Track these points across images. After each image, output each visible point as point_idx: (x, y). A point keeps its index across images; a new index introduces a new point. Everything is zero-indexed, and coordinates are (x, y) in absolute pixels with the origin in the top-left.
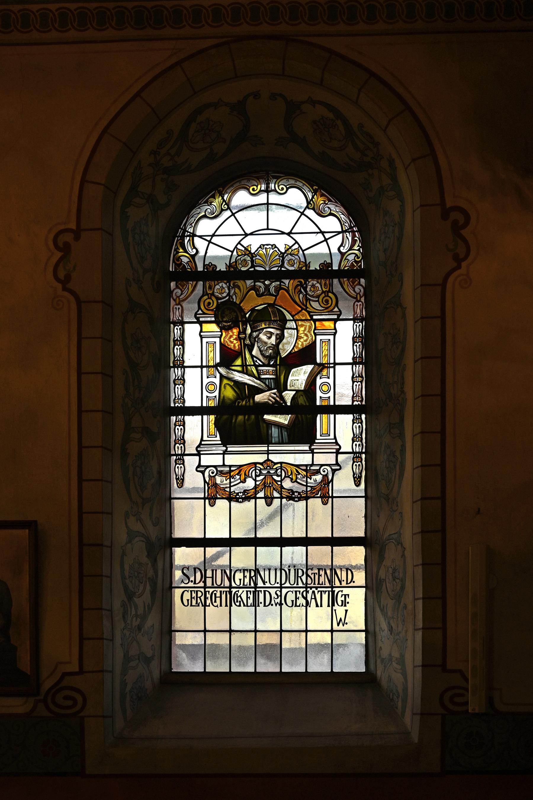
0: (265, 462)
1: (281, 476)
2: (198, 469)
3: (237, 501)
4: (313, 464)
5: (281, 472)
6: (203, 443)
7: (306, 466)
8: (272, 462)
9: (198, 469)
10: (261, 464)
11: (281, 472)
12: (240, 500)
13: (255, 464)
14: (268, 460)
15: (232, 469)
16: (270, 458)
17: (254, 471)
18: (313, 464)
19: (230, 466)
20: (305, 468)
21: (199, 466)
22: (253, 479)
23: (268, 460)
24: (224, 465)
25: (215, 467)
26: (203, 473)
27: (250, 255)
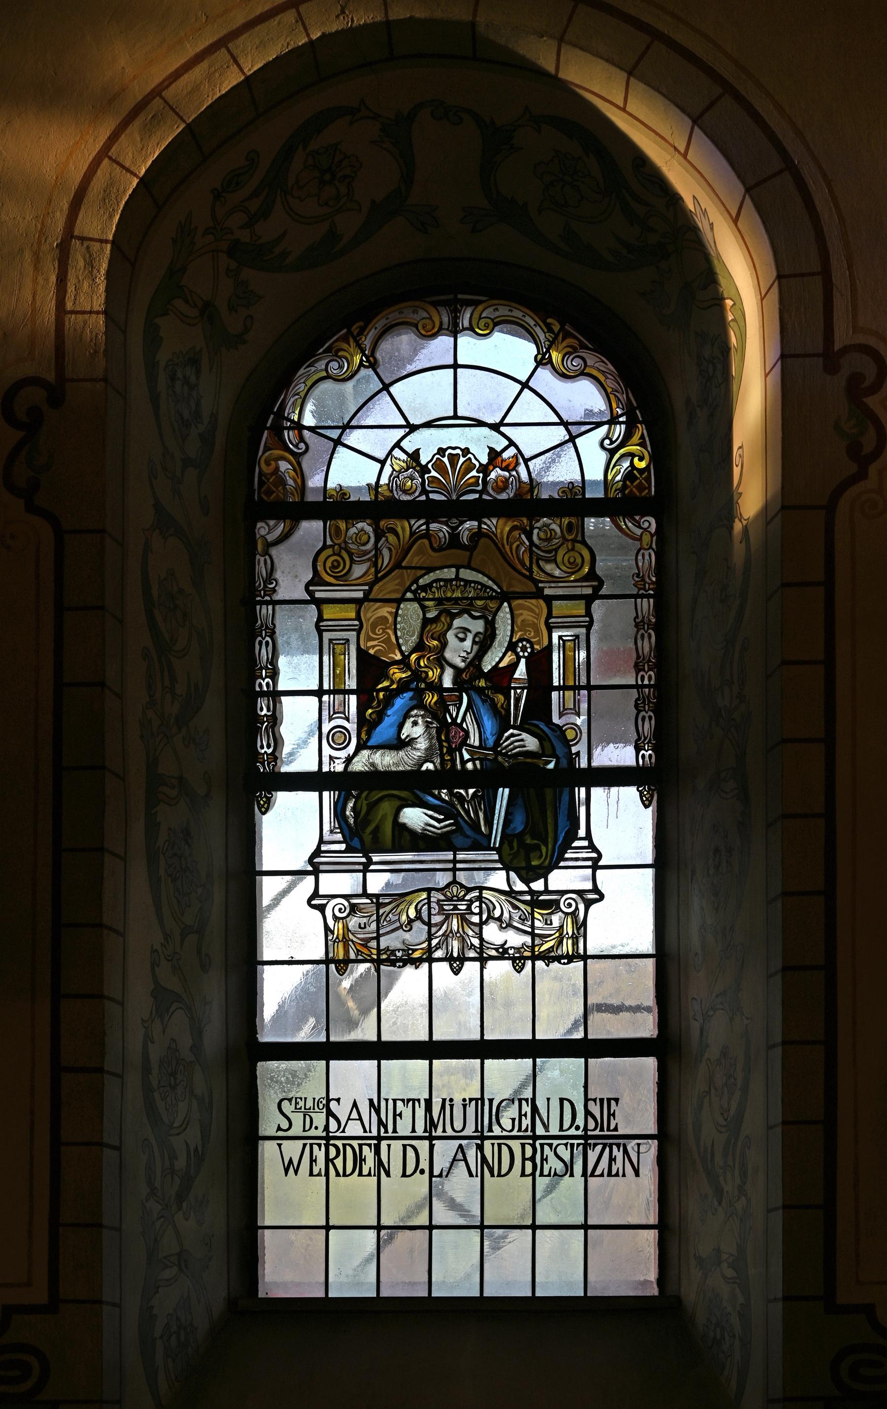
8: (462, 886)
14: (454, 882)
17: (426, 906)
19: (377, 896)
21: (316, 894)
23: (454, 882)
26: (321, 909)
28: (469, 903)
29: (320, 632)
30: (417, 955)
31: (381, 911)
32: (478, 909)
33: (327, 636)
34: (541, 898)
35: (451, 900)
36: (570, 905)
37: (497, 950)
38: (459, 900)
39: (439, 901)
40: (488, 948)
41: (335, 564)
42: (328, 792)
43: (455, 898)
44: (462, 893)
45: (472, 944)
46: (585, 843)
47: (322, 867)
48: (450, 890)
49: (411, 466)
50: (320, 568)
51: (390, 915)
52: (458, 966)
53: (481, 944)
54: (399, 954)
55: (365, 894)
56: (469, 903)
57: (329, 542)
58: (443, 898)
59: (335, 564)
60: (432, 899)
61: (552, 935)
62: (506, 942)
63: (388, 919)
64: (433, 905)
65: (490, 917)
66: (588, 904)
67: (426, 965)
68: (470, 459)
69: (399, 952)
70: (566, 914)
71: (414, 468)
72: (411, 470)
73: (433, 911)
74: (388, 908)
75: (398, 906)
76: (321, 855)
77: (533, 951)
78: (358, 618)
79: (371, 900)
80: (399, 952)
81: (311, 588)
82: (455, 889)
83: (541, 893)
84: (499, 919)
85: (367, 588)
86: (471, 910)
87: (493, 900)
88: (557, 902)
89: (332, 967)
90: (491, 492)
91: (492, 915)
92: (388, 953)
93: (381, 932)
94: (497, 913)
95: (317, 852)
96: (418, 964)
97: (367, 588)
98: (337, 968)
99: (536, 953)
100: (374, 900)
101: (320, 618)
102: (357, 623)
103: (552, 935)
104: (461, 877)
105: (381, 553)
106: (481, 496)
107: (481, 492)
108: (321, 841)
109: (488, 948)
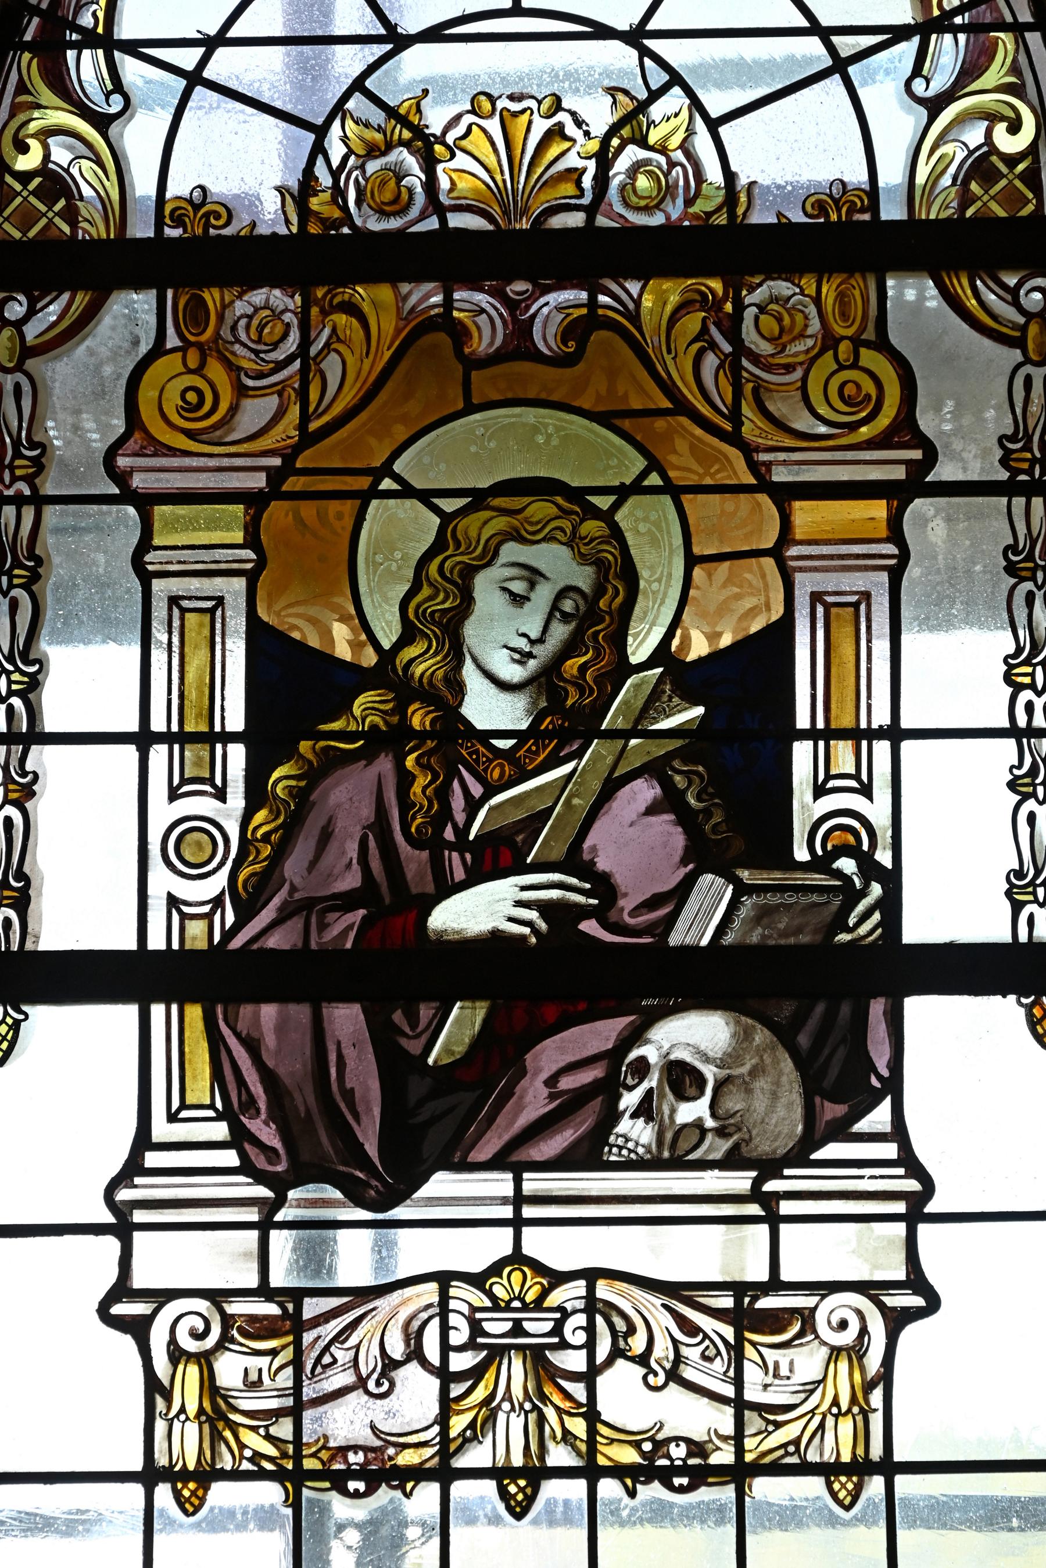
0: (496, 1269)
1: (590, 1346)
2: (117, 1309)
3: (338, 1482)
4: (775, 1284)
5: (590, 1329)
7: (739, 1289)
8: (539, 1268)
9: (117, 1309)
10: (477, 1280)
11: (590, 1329)
13: (444, 1279)
14: (518, 1258)
16: (527, 1250)
17: (436, 1321)
18: (775, 1284)
21: (122, 1290)
23: (518, 1258)
24: (264, 1291)
25: (216, 1296)
28: (558, 1315)
34: (766, 1303)
35: (508, 1308)
36: (843, 1325)
37: (637, 1445)
40: (612, 1441)
43: (516, 1304)
46: (889, 1150)
47: (139, 1216)
52: (521, 1490)
53: (592, 1432)
64: (454, 1319)
65: (617, 1353)
79: (281, 1305)
80: (356, 1453)
84: (643, 1360)
89: (163, 1493)
92: (324, 1455)
93: (309, 1392)
94: (638, 1344)
98: (177, 1495)
100: (290, 1307)
109: (612, 1441)
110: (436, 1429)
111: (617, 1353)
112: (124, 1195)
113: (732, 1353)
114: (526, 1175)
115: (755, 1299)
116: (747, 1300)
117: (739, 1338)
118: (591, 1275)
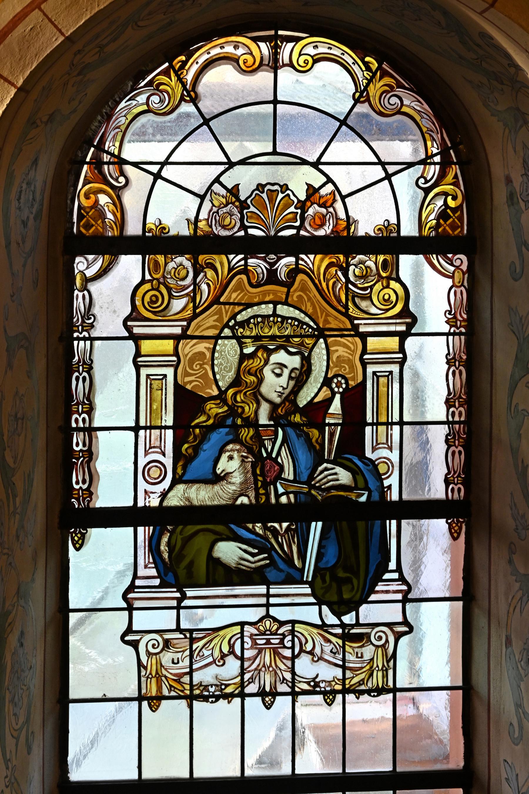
0: (261, 620)
1: (293, 648)
5: (293, 641)
6: (138, 583)
8: (275, 620)
11: (293, 641)
12: (210, 700)
13: (242, 624)
14: (268, 615)
15: (194, 636)
17: (239, 640)
19: (191, 631)
20: (339, 631)
21: (129, 630)
22: (236, 657)
23: (268, 615)
27: (237, 204)
28: (281, 637)
29: (138, 367)
30: (229, 690)
31: (195, 646)
32: (290, 643)
33: (144, 372)
35: (264, 634)
36: (380, 638)
37: (308, 683)
38: (271, 634)
39: (252, 635)
40: (300, 682)
41: (154, 299)
42: (143, 528)
44: (275, 627)
45: (284, 679)
48: (264, 625)
49: (230, 201)
50: (138, 303)
51: (204, 650)
52: (270, 700)
53: (293, 678)
54: (212, 689)
55: (178, 629)
56: (281, 637)
57: (148, 277)
58: (256, 632)
59: (154, 299)
60: (245, 634)
61: (362, 668)
62: (317, 676)
63: (201, 654)
64: (246, 639)
66: (398, 636)
67: (237, 701)
68: (288, 195)
69: (212, 687)
70: (377, 647)
71: (233, 203)
72: (231, 205)
73: (246, 646)
74: (201, 643)
75: (211, 641)
76: (136, 590)
77: (344, 684)
78: (176, 353)
80: (212, 687)
81: (129, 323)
82: (268, 623)
83: (352, 626)
84: (311, 653)
85: (185, 323)
86: (283, 644)
87: (306, 634)
88: (368, 635)
89: (145, 704)
90: (308, 228)
91: (304, 648)
92: (201, 688)
93: (195, 667)
94: (309, 647)
95: (132, 588)
96: (230, 699)
97: (185, 323)
98: (149, 705)
99: (347, 686)
101: (138, 354)
102: (174, 358)
103: (362, 668)
104: (273, 611)
105: (199, 288)
106: (298, 232)
107: (299, 228)
108: (135, 576)
109: (300, 682)
110: (239, 678)
111: (301, 651)
112: (131, 595)
113: (341, 649)
114: (271, 587)
115: (350, 630)
116: (346, 631)
117: (344, 644)
118: (293, 622)
